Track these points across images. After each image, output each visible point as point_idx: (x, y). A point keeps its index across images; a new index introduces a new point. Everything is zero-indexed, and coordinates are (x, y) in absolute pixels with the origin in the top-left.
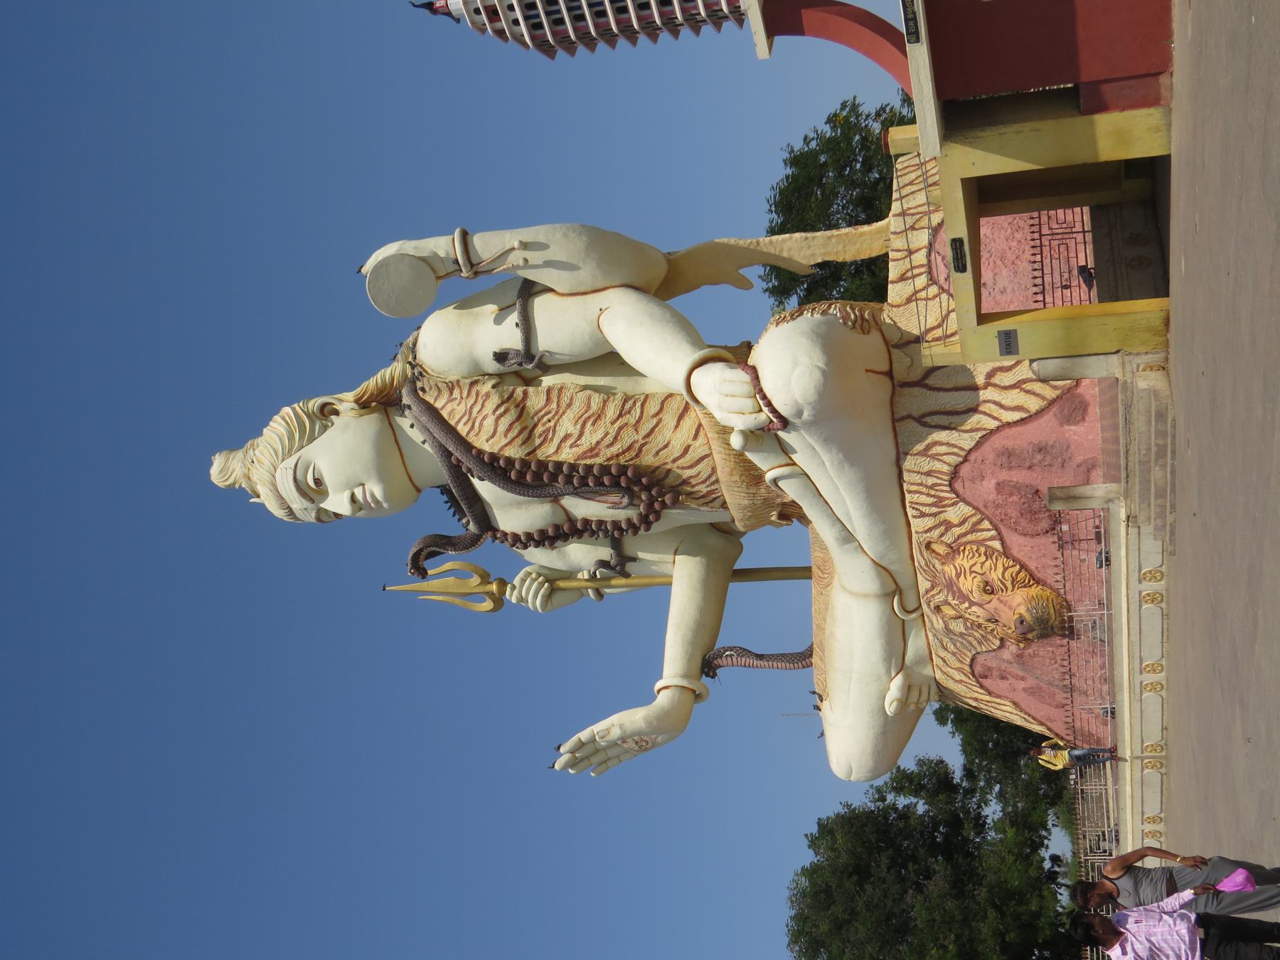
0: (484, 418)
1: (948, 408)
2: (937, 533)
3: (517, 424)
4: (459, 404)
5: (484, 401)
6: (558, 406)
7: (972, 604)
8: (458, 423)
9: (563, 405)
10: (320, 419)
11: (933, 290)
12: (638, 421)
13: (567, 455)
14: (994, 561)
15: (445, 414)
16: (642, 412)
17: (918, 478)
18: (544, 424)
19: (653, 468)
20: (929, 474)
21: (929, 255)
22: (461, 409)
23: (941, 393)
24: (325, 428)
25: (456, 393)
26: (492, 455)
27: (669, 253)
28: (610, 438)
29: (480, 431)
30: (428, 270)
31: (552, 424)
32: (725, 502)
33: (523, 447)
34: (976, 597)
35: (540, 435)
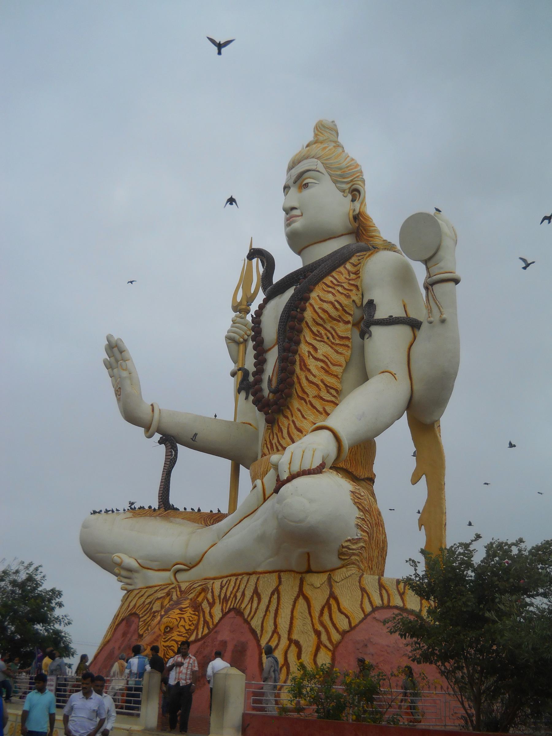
0: (333, 294)
1: (280, 611)
2: (209, 596)
3: (327, 316)
4: (346, 278)
5: (345, 295)
6: (337, 344)
7: (162, 617)
8: (333, 277)
9: (337, 348)
10: (350, 188)
11: (368, 609)
12: (321, 398)
13: (304, 349)
14: (184, 635)
15: (341, 269)
16: (328, 401)
17: (242, 587)
18: (326, 334)
19: (290, 407)
20: (243, 594)
21: (396, 607)
22: (342, 279)
23: (291, 607)
24: (343, 191)
25: (353, 276)
26: (308, 299)
27: (439, 426)
28: (311, 378)
29: (325, 291)
30: (431, 254)
31: (326, 340)
32: (265, 455)
33: (311, 320)
34: (165, 620)
35: (318, 332)
